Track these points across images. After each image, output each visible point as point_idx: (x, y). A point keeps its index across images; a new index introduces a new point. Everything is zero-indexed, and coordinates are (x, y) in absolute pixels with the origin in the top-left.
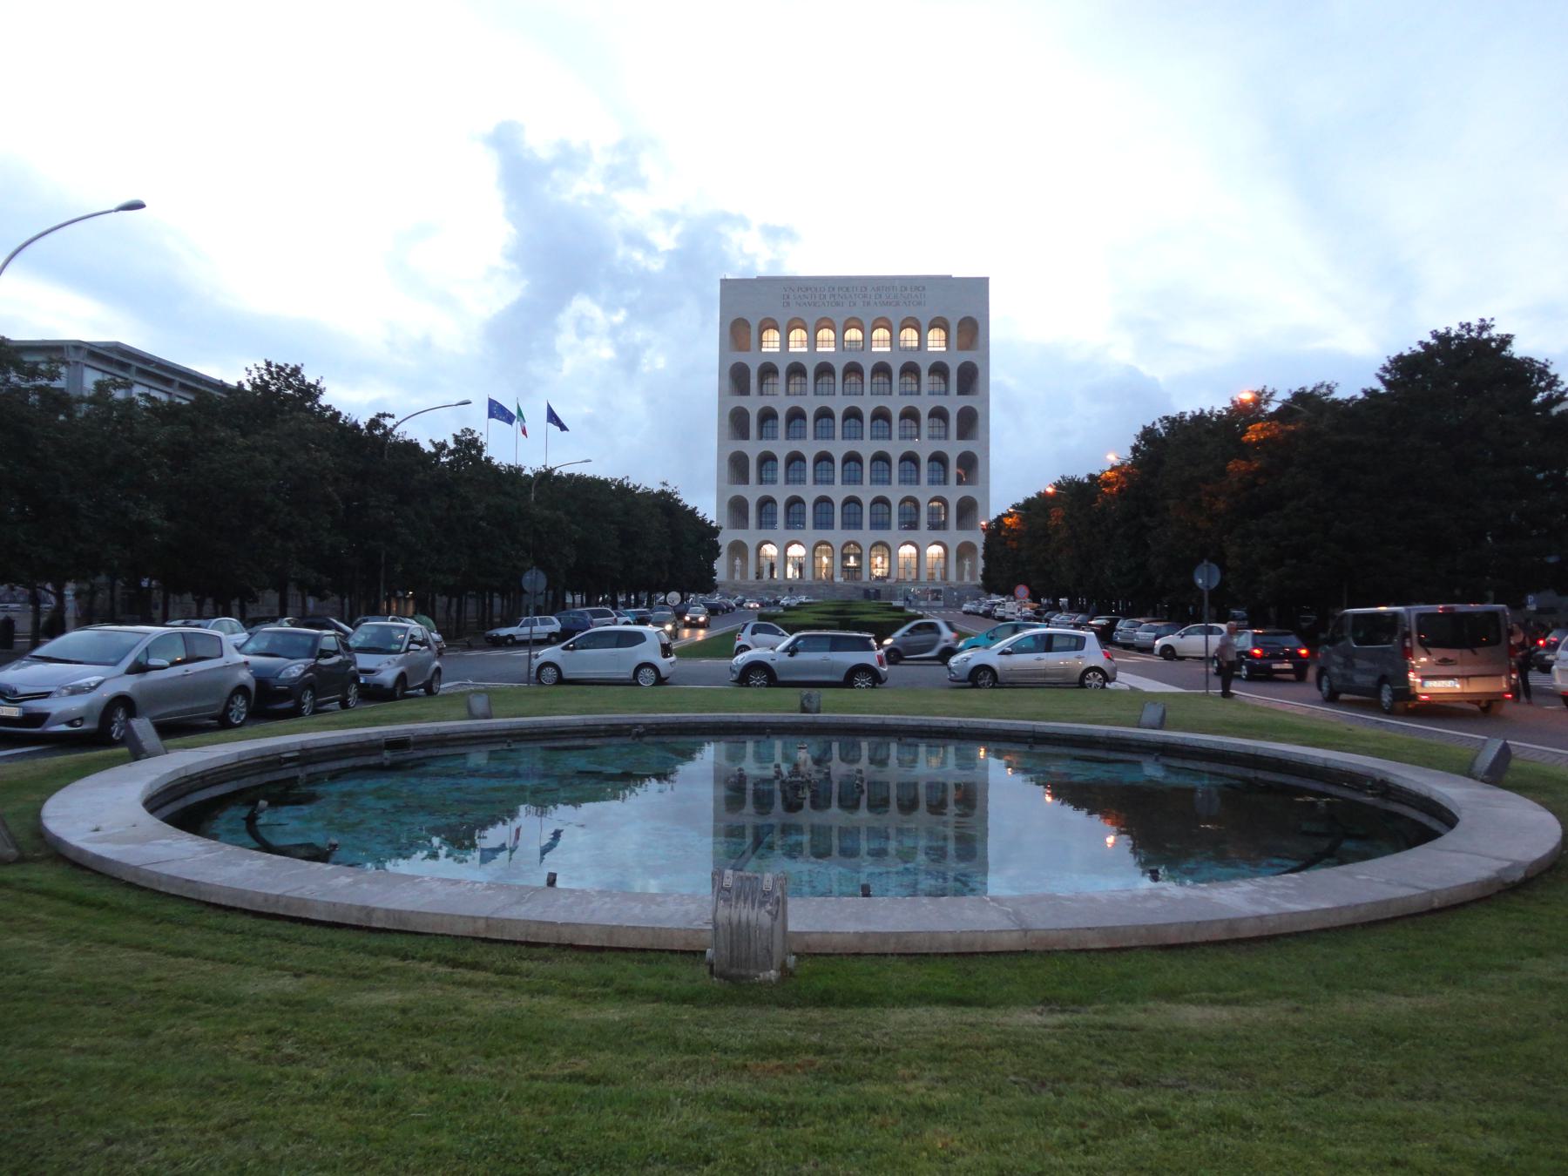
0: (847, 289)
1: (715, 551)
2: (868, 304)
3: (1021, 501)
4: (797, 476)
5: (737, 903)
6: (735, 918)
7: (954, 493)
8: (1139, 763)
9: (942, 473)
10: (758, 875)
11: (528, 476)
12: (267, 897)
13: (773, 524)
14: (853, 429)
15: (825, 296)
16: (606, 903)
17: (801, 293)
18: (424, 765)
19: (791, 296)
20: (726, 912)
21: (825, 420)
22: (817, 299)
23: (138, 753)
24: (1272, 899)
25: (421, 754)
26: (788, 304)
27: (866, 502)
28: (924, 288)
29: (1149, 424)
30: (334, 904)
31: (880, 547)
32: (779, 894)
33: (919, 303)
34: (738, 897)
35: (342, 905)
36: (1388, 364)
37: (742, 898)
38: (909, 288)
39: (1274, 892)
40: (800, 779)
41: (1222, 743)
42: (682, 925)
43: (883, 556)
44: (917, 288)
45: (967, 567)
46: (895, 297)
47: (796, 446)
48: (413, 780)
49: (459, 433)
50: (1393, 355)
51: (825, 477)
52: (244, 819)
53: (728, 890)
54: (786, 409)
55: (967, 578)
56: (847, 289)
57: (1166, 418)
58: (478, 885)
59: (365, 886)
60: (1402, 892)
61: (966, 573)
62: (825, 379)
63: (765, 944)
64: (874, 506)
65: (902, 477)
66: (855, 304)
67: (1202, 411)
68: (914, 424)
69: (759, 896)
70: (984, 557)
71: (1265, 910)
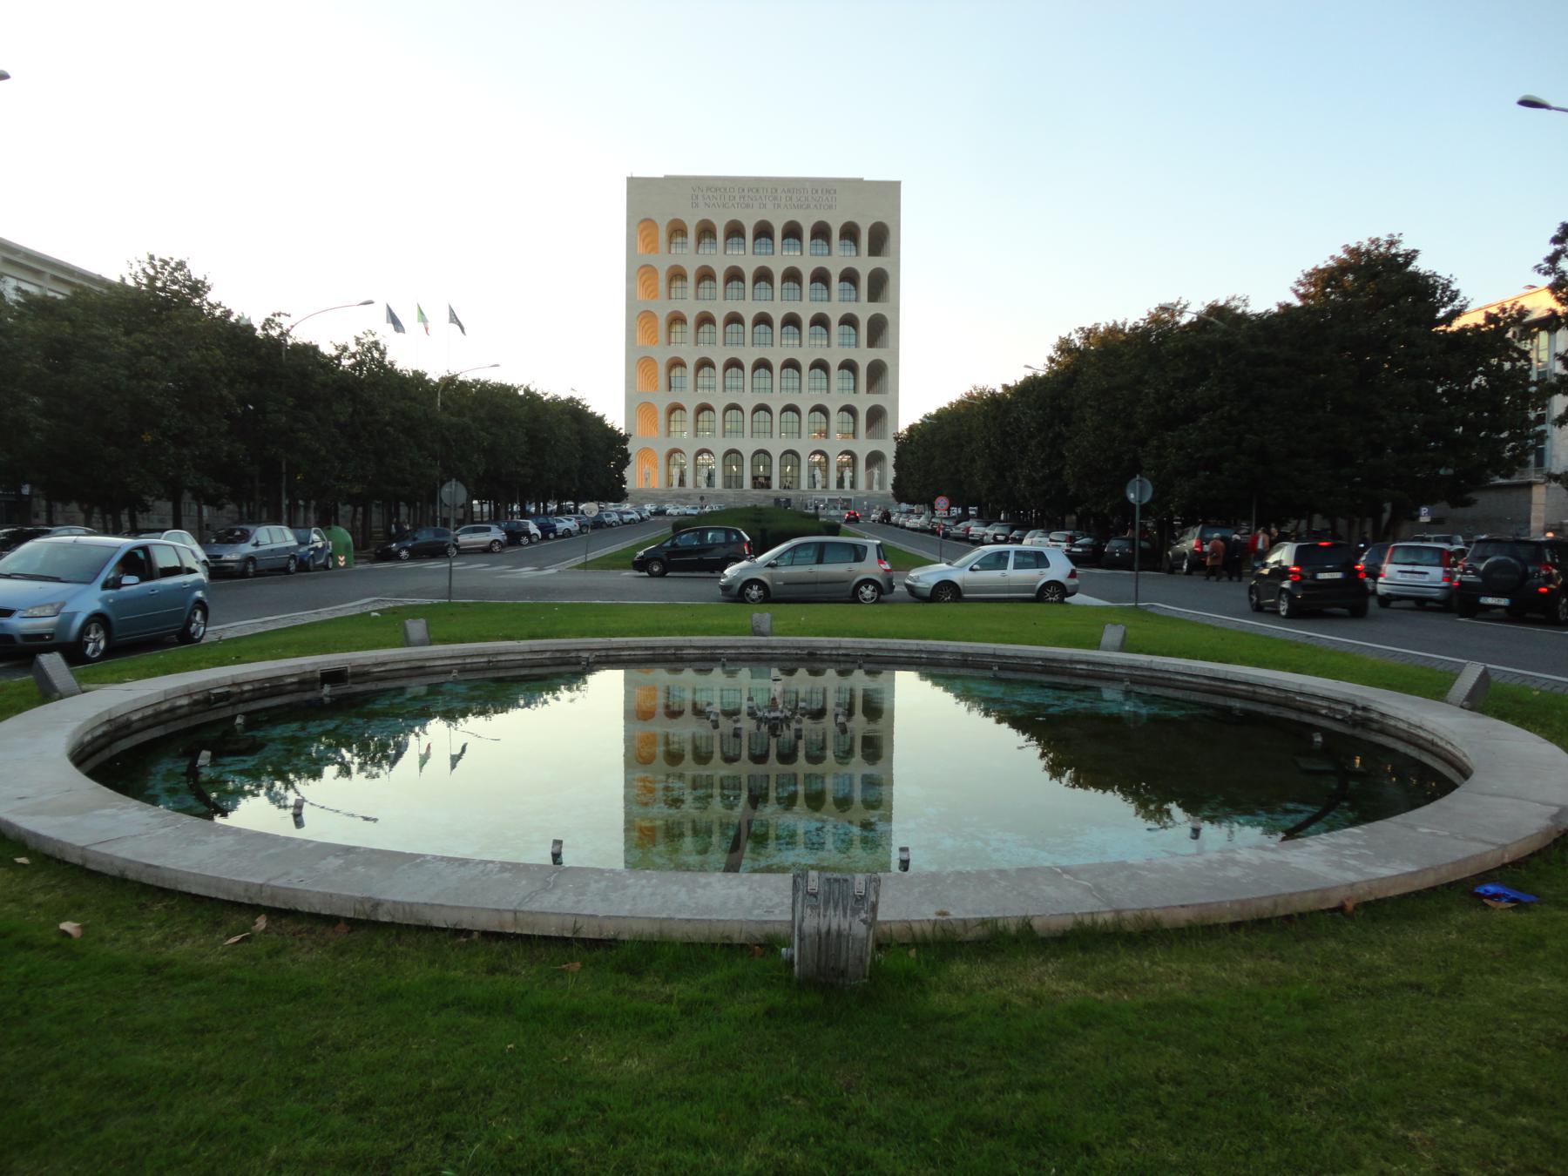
1: (625, 459)
2: (779, 206)
3: (934, 412)
4: (706, 383)
5: (826, 910)
6: (824, 930)
7: (864, 402)
8: (1098, 689)
9: (852, 381)
10: (848, 877)
11: (430, 380)
12: (248, 886)
14: (763, 336)
16: (643, 887)
17: (711, 194)
18: (367, 701)
19: (700, 198)
20: (815, 923)
21: (735, 325)
23: (47, 693)
24: (1352, 862)
25: (360, 688)
26: (697, 205)
27: (776, 410)
29: (1065, 335)
30: (331, 895)
31: (789, 456)
32: (873, 899)
33: (830, 207)
34: (827, 903)
35: (339, 896)
36: (1302, 278)
37: (831, 904)
38: (820, 192)
39: (1348, 852)
40: (778, 714)
41: (1190, 667)
42: (741, 917)
43: (792, 466)
44: (828, 191)
45: (876, 476)
46: (807, 199)
47: (706, 352)
48: (360, 722)
49: (360, 335)
50: (1309, 269)
51: (734, 384)
52: (184, 774)
53: (815, 895)
54: (695, 313)
55: (876, 487)
57: (1082, 329)
58: (490, 865)
59: (361, 869)
60: (1475, 848)
61: (875, 482)
62: (735, 283)
63: (858, 954)
65: (812, 385)
66: (765, 206)
67: (1115, 323)
68: (824, 331)
69: (851, 902)
70: (895, 466)
71: (1351, 877)
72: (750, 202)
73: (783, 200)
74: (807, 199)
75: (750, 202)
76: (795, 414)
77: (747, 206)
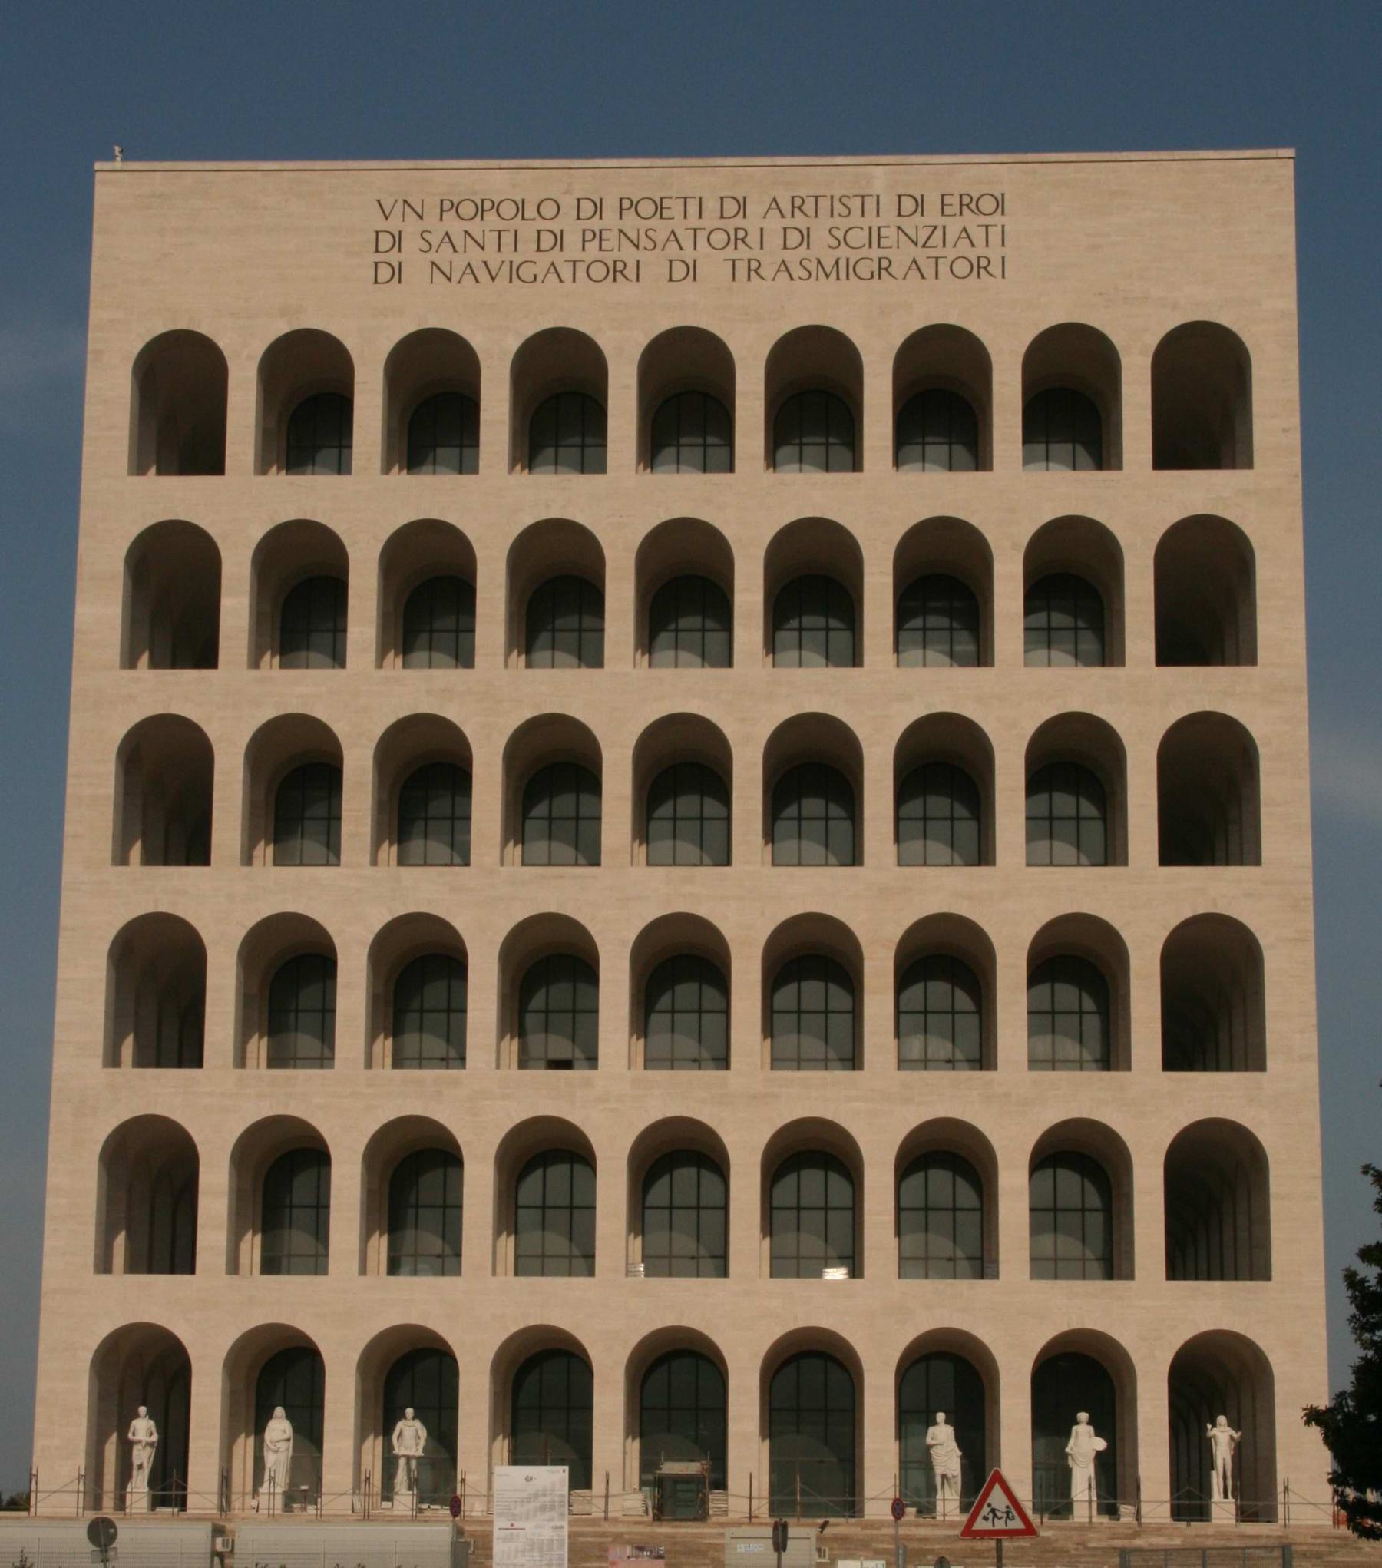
0: (659, 208)
2: (754, 270)
13: (317, 1263)
15: (559, 239)
17: (456, 228)
19: (412, 243)
22: (527, 249)
26: (397, 272)
28: (1000, 204)
33: (979, 267)
44: (969, 204)
46: (876, 237)
56: (659, 208)
64: (789, 1181)
66: (692, 270)
72: (629, 254)
73: (774, 241)
74: (876, 237)
75: (629, 254)
76: (835, 1178)
77: (615, 271)
